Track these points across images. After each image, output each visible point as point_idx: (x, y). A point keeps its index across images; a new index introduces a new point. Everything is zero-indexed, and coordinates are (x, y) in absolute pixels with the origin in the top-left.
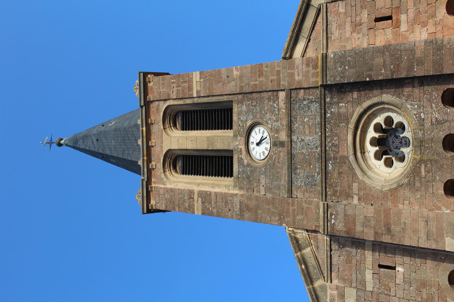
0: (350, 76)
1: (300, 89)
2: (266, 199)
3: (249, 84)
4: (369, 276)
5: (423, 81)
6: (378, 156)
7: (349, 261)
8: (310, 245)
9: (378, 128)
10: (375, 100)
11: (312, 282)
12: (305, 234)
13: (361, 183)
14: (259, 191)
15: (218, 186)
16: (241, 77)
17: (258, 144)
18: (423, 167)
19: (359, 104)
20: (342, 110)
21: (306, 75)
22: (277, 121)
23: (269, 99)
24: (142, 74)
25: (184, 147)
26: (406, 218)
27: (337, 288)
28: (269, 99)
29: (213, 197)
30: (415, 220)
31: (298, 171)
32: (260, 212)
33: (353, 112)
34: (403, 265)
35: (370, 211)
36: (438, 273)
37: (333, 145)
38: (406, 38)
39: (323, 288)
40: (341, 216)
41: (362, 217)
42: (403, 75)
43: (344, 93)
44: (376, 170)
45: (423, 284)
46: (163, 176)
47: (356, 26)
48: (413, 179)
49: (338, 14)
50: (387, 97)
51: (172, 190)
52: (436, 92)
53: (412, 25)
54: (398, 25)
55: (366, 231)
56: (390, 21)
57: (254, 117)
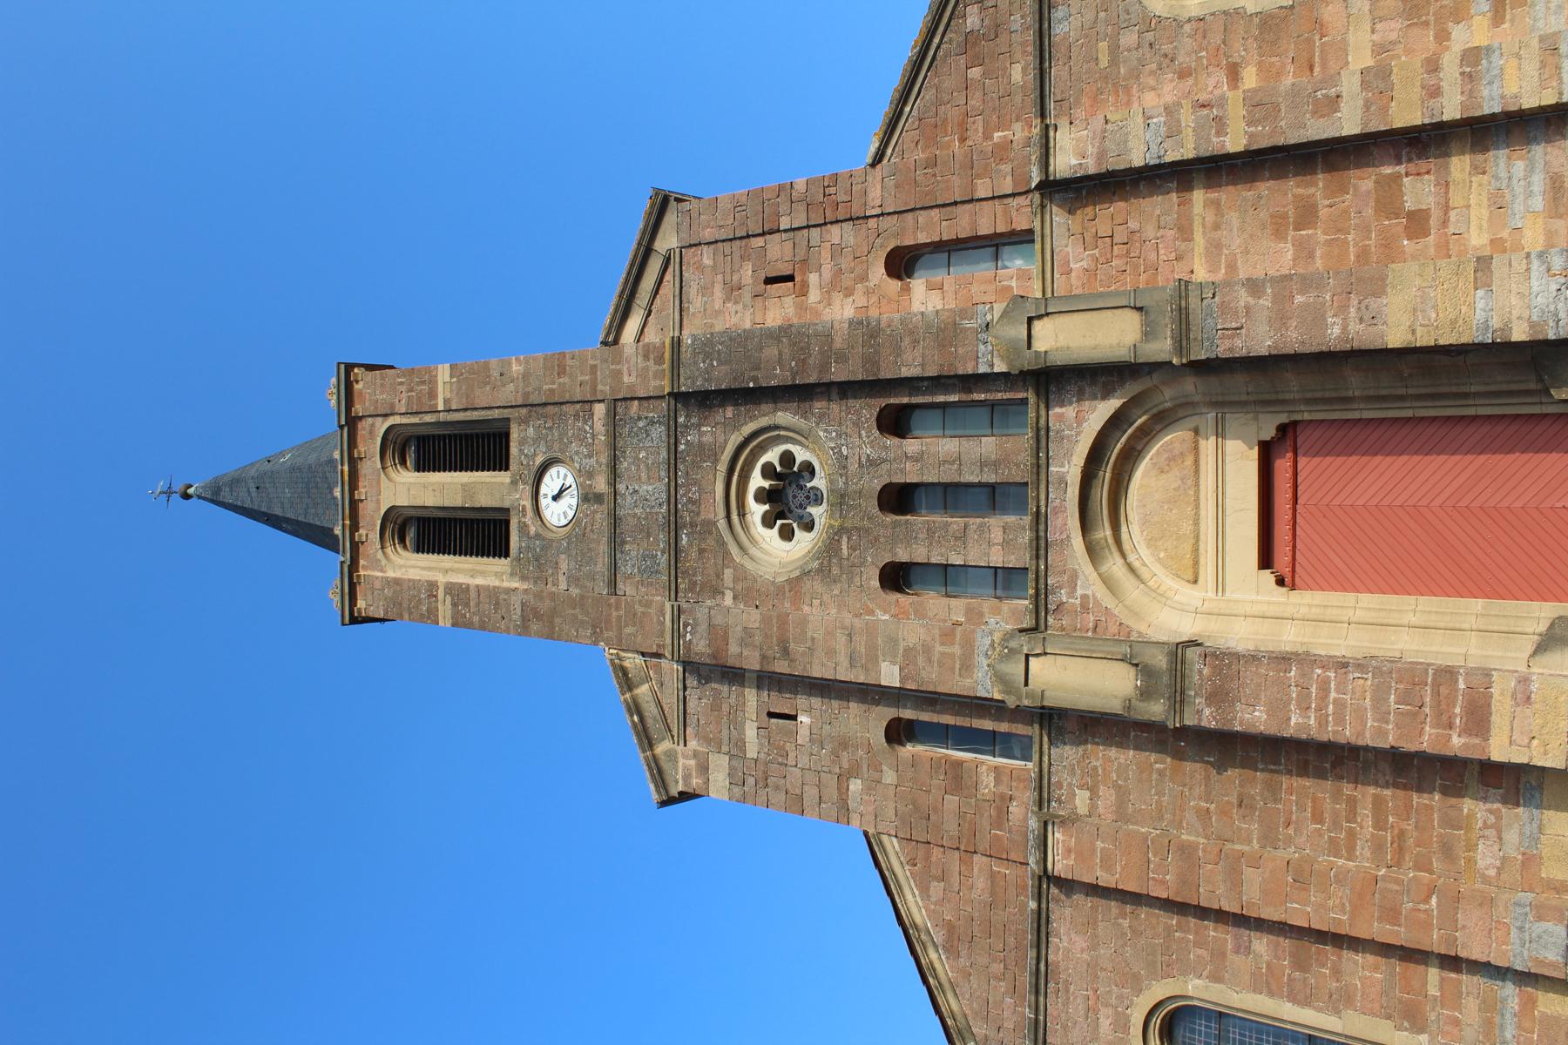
0: (721, 379)
1: (633, 399)
2: (570, 596)
4: (751, 732)
5: (847, 390)
6: (768, 521)
7: (715, 707)
8: (648, 679)
9: (768, 471)
10: (764, 422)
11: (651, 746)
12: (639, 660)
14: (556, 584)
15: (483, 573)
16: (526, 376)
17: (555, 498)
18: (845, 539)
19: (736, 428)
20: (707, 439)
21: (643, 374)
22: (590, 456)
23: (577, 416)
25: (419, 503)
26: (815, 630)
27: (696, 754)
28: (577, 416)
29: (473, 594)
30: (830, 633)
31: (627, 547)
32: (557, 620)
33: (726, 442)
34: (809, 711)
35: (753, 618)
36: (868, 724)
37: (690, 500)
38: (818, 314)
39: (672, 756)
40: (703, 628)
41: (739, 628)
42: (812, 380)
43: (710, 407)
44: (764, 546)
45: (844, 744)
47: (733, 290)
48: (827, 561)
49: (700, 268)
50: (784, 417)
51: (397, 582)
53: (828, 292)
54: (803, 292)
55: (745, 653)
56: (790, 284)
57: (549, 448)
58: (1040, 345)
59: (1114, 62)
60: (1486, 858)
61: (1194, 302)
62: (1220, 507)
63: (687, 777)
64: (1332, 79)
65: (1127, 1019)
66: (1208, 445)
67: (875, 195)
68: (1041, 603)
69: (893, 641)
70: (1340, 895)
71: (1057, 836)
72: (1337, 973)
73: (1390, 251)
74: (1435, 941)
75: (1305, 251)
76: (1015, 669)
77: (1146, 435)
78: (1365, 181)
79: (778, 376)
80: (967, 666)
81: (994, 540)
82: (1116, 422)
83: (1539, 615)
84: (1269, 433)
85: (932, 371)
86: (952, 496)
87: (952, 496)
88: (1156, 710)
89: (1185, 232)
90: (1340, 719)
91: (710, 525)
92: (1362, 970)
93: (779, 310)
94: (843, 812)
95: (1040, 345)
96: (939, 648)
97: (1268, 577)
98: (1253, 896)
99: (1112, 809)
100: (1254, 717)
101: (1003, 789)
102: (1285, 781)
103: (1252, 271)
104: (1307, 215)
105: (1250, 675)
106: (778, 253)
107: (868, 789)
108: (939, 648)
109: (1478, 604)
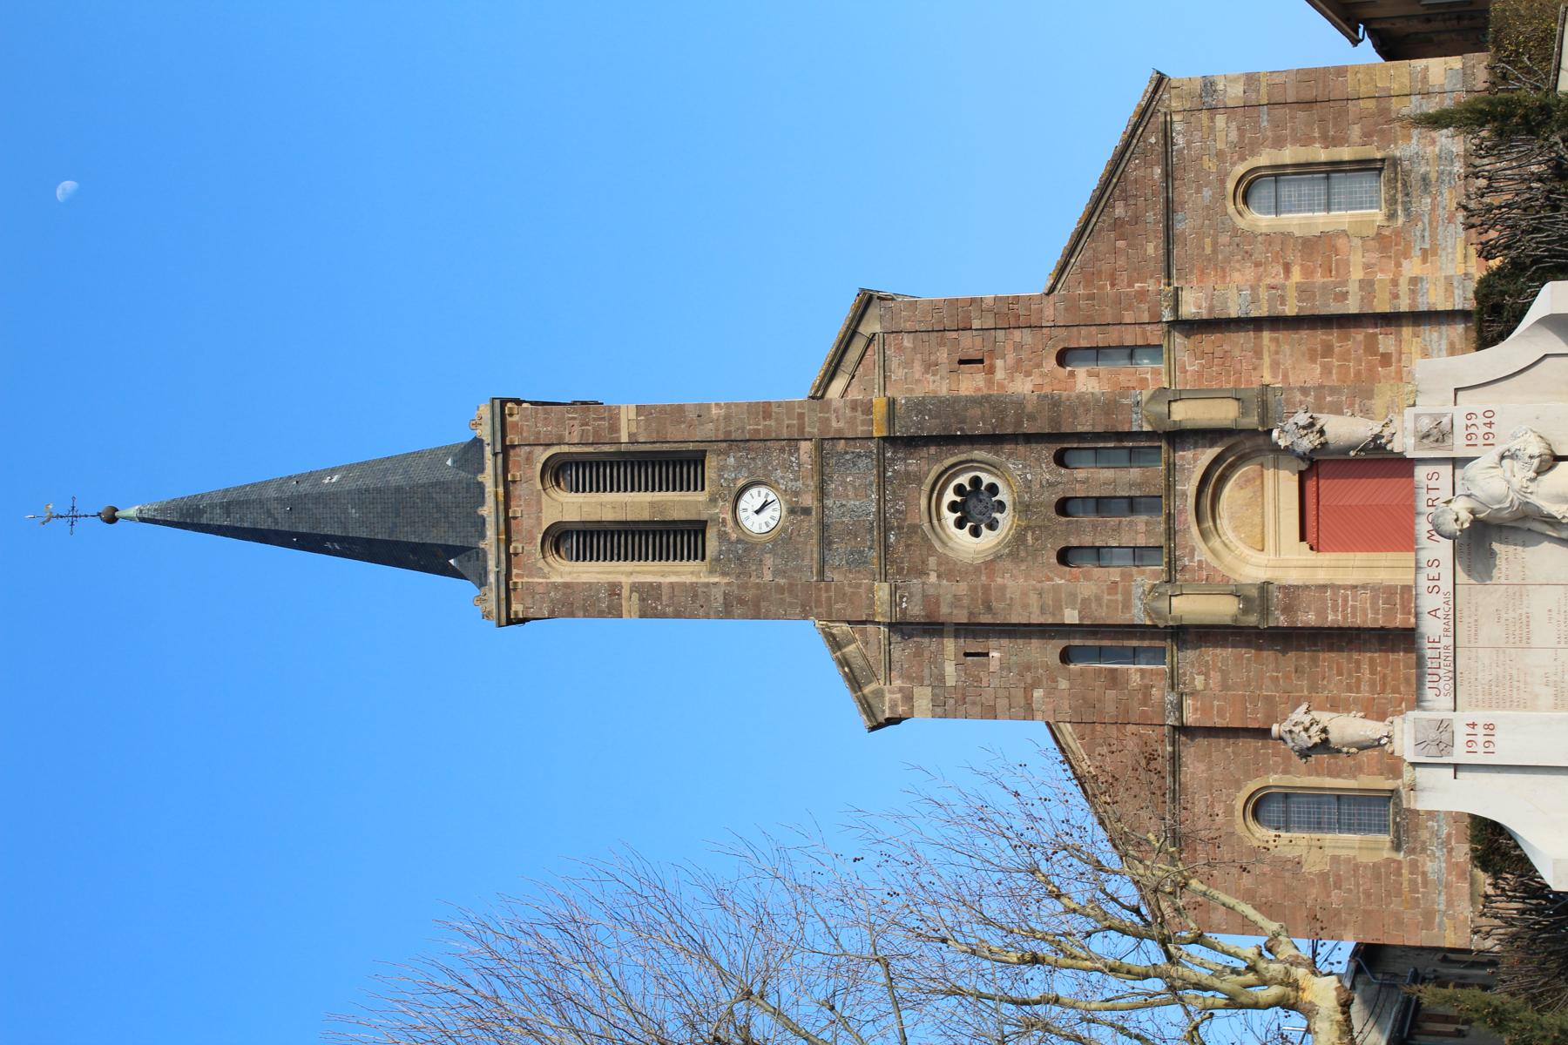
0: (932, 427)
2: (778, 585)
3: (743, 429)
4: (950, 668)
5: (1029, 438)
6: (960, 524)
7: (918, 653)
8: (854, 641)
9: (959, 490)
10: (963, 457)
11: (860, 689)
12: (846, 627)
13: (939, 556)
16: (727, 418)
21: (852, 422)
23: (782, 450)
24: (497, 403)
27: (901, 690)
28: (782, 450)
30: (1025, 594)
32: (763, 604)
35: (962, 588)
37: (898, 511)
38: (1001, 386)
39: (879, 694)
40: (918, 597)
42: (1009, 431)
43: (916, 447)
45: (1028, 668)
46: (541, 563)
47: (930, 367)
48: (1016, 547)
49: (900, 348)
50: (979, 454)
51: (567, 585)
54: (991, 370)
57: (751, 473)
58: (1176, 417)
59: (1215, 251)
61: (1270, 397)
63: (893, 707)
64: (1344, 283)
65: (1233, 807)
66: (1269, 473)
67: (1049, 313)
68: (1172, 566)
69: (1073, 595)
71: (1188, 702)
73: (1373, 378)
75: (1327, 370)
76: (1162, 605)
77: (1232, 467)
78: (1359, 335)
79: (981, 428)
80: (1127, 606)
81: (1140, 530)
82: (1217, 461)
85: (1099, 429)
86: (1101, 505)
88: (1252, 620)
89: (1258, 354)
90: (1354, 616)
91: (915, 528)
93: (970, 384)
94: (1029, 713)
95: (1176, 417)
96: (1106, 597)
97: (1305, 545)
100: (1308, 618)
101: (1146, 681)
102: (1321, 655)
104: (1328, 351)
105: (1304, 595)
106: (969, 344)
107: (1048, 694)
108: (1106, 597)
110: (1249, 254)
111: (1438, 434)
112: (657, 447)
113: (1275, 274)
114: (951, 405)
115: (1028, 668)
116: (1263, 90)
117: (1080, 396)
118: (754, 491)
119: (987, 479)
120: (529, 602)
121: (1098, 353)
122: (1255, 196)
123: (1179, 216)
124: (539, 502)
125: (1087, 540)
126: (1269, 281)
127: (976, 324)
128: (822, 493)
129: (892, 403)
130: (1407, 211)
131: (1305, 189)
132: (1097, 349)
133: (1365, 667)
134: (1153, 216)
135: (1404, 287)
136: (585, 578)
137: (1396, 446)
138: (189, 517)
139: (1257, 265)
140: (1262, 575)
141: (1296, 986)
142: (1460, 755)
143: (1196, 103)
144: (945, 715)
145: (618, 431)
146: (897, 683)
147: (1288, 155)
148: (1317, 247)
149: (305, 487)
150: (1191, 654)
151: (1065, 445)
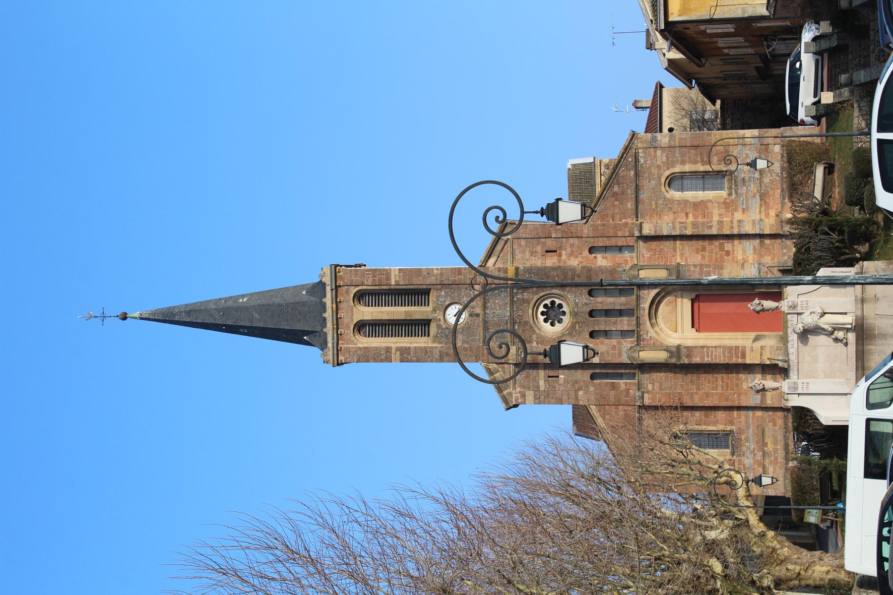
4: (542, 383)
5: (577, 285)
6: (546, 321)
8: (499, 371)
9: (545, 306)
10: (548, 292)
12: (495, 365)
13: (537, 335)
16: (441, 274)
23: (466, 289)
27: (520, 392)
38: (564, 262)
39: (510, 394)
46: (353, 338)
47: (533, 253)
49: (520, 245)
50: (554, 291)
51: (366, 348)
52: (585, 291)
54: (560, 255)
58: (641, 276)
59: (656, 207)
60: (745, 386)
62: (682, 314)
63: (517, 400)
64: (711, 222)
66: (679, 300)
67: (585, 231)
70: (716, 398)
71: (646, 396)
72: (715, 417)
73: (722, 260)
74: (736, 404)
75: (703, 257)
77: (664, 297)
78: (717, 243)
80: (620, 355)
81: (625, 323)
83: (753, 335)
84: (693, 297)
86: (608, 313)
87: (608, 313)
88: (673, 361)
89: (675, 250)
91: (526, 323)
92: (721, 415)
93: (551, 261)
95: (641, 276)
97: (694, 330)
98: (697, 402)
99: (656, 388)
100: (697, 360)
103: (692, 261)
104: (704, 249)
106: (550, 244)
107: (585, 393)
109: (740, 333)
110: (671, 209)
111: (794, 307)
112: (409, 287)
113: (682, 218)
114: (543, 271)
115: (576, 382)
116: (677, 141)
117: (600, 267)
118: (453, 306)
119: (558, 301)
120: (347, 356)
121: (606, 249)
122: (673, 185)
123: (641, 192)
124: (352, 311)
125: (602, 328)
126: (679, 220)
127: (554, 235)
128: (485, 307)
129: (517, 269)
130: (736, 193)
131: (694, 182)
132: (606, 247)
133: (720, 380)
134: (630, 192)
135: (735, 224)
136: (374, 345)
137: (782, 309)
138: (168, 317)
139: (675, 213)
140: (676, 342)
141: (731, 477)
142: (800, 391)
143: (649, 145)
144: (539, 403)
145: (390, 280)
146: (518, 389)
147: (687, 168)
148: (699, 206)
149: (229, 304)
150: (646, 376)
151: (594, 288)
